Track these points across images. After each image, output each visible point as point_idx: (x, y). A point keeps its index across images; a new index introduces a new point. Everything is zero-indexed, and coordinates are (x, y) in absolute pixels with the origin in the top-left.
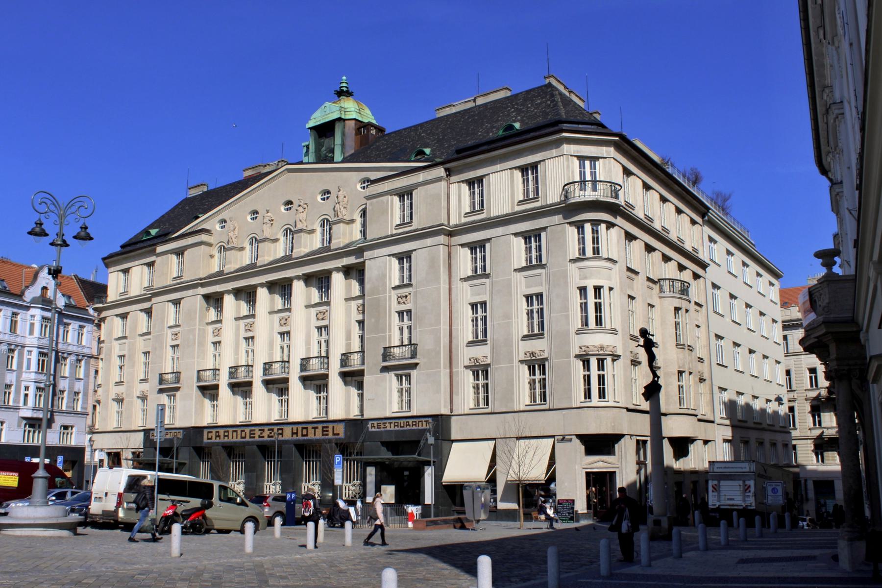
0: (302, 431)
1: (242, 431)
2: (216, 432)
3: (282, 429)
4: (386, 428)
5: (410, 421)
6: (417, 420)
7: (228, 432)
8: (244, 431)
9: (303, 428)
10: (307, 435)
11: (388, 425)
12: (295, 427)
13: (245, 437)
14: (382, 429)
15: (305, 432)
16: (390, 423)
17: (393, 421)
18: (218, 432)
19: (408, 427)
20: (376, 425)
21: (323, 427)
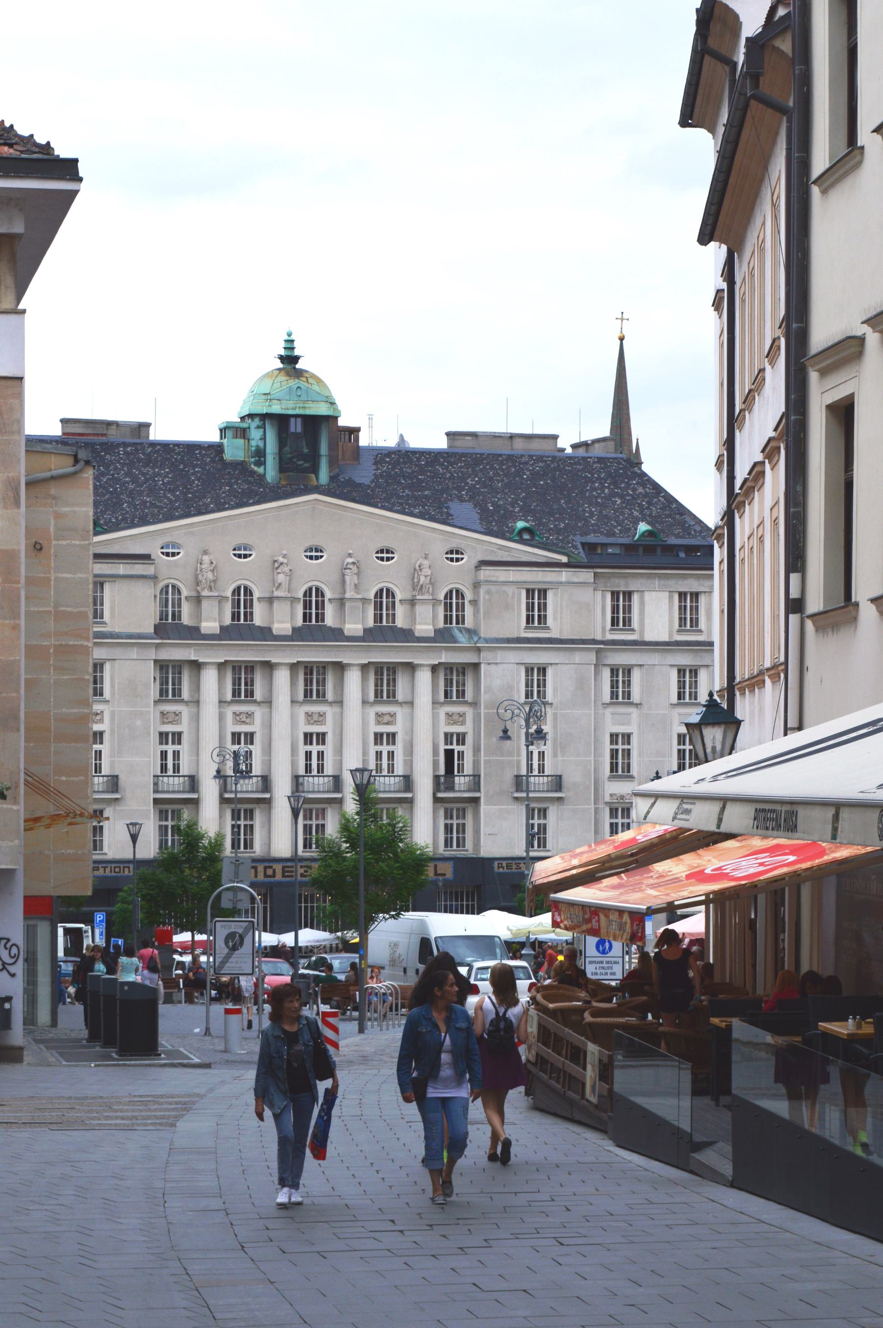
1: (265, 868)
4: (520, 868)
13: (274, 876)
14: (514, 870)
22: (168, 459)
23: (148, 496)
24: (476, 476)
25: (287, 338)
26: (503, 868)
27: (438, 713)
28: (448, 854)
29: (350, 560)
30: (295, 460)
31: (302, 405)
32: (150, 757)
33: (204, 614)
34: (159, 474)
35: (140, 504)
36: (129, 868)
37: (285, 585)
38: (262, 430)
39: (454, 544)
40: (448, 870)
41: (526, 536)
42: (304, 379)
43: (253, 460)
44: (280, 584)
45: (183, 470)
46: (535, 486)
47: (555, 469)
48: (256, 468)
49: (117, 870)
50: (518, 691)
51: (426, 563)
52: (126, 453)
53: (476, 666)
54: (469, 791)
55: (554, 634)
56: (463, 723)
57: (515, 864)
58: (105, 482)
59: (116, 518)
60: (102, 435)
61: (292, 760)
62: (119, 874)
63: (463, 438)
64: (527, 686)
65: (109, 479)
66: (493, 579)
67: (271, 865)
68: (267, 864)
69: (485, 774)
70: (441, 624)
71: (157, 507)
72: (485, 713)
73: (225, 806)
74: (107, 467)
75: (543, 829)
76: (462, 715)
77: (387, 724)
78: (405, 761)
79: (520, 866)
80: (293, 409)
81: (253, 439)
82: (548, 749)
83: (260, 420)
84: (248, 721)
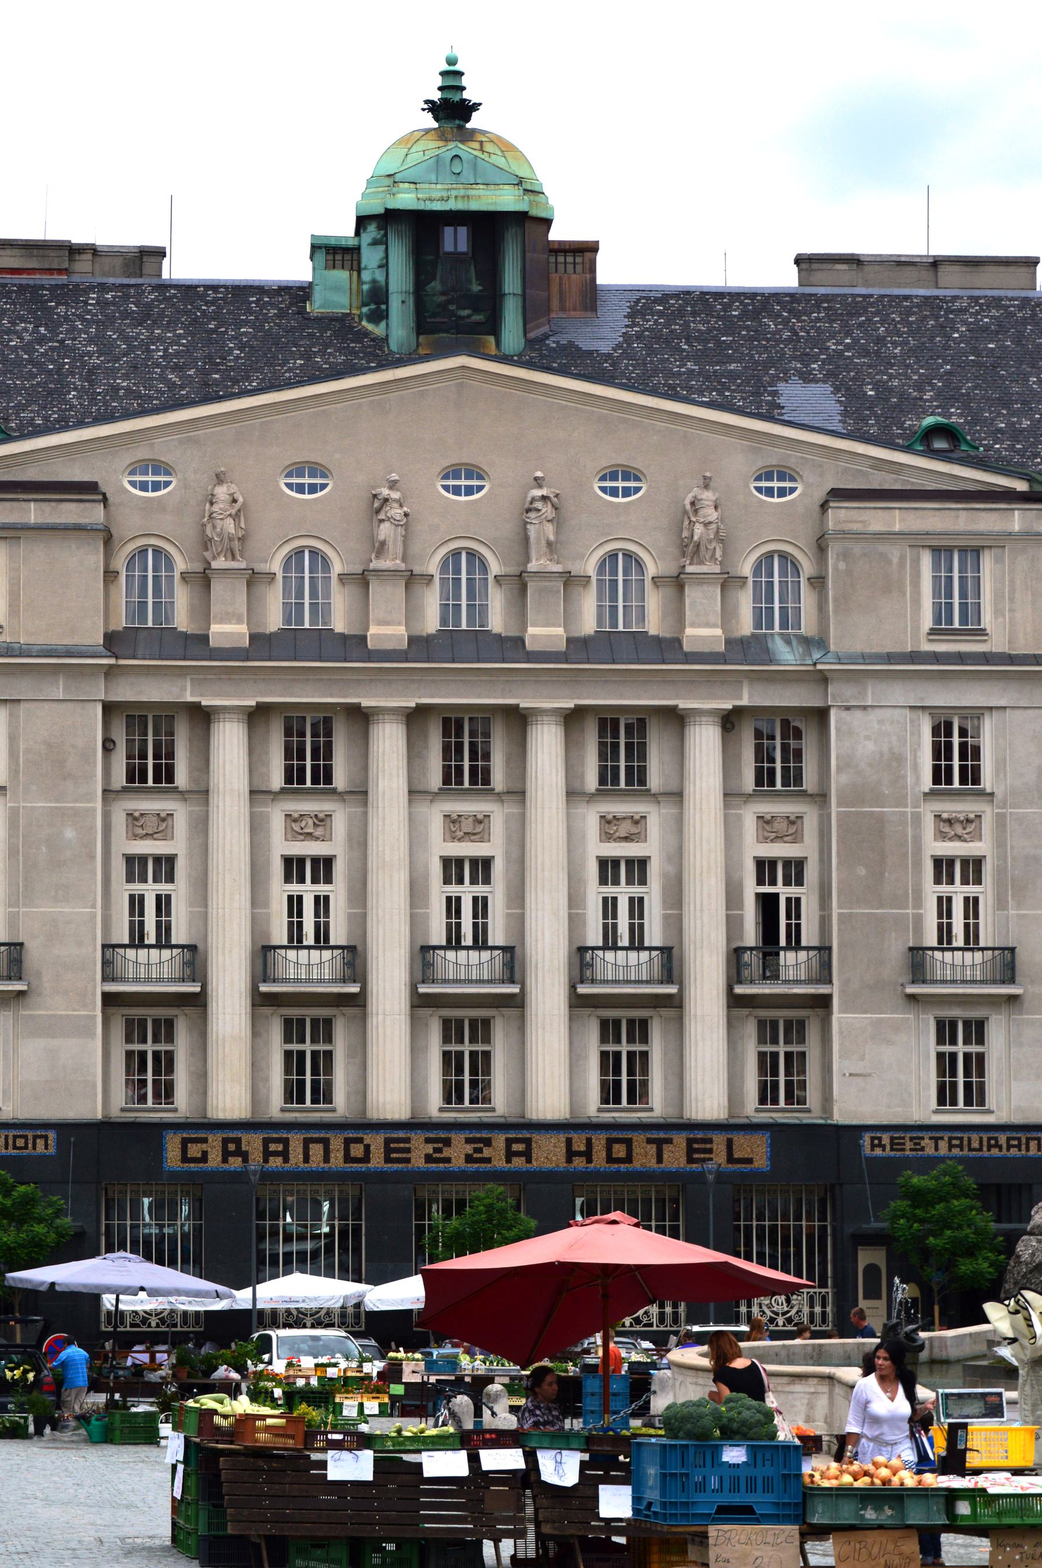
1: (348, 1142)
2: (225, 1142)
3: (528, 1142)
4: (923, 1149)
6: (1023, 1136)
7: (286, 1142)
9: (610, 1143)
10: (629, 1159)
11: (926, 1142)
13: (366, 1159)
14: (908, 1153)
15: (619, 1151)
16: (936, 1140)
17: (946, 1135)
18: (238, 1141)
19: (995, 1152)
21: (690, 1142)
22: (187, 312)
23: (126, 377)
24: (848, 334)
25: (446, 67)
26: (884, 1147)
27: (739, 817)
28: (764, 1117)
29: (538, 493)
30: (452, 307)
31: (462, 192)
32: (94, 906)
33: (215, 608)
34: (160, 339)
35: (106, 393)
36: (46, 1138)
37: (395, 547)
38: (383, 247)
39: (773, 457)
41: (940, 444)
42: (476, 145)
43: (365, 310)
44: (383, 544)
45: (213, 331)
46: (975, 351)
47: (1024, 321)
48: (370, 327)
49: (20, 1142)
50: (916, 767)
51: (708, 496)
52: (101, 303)
53: (821, 715)
54: (809, 981)
55: (996, 644)
56: (797, 838)
57: (911, 1139)
58: (42, 354)
59: (46, 419)
60: (60, 271)
61: (412, 916)
62: (25, 1152)
63: (830, 266)
64: (936, 756)
65: (52, 348)
66: (856, 527)
67: (360, 1135)
68: (351, 1135)
69: (840, 945)
70: (746, 626)
71: (139, 396)
72: (839, 813)
73: (267, 1011)
74: (53, 329)
75: (976, 1064)
76: (794, 821)
77: (626, 839)
78: (666, 918)
79: (923, 1143)
80: (442, 199)
81: (365, 268)
82: (985, 892)
83: (379, 228)
84: (319, 832)
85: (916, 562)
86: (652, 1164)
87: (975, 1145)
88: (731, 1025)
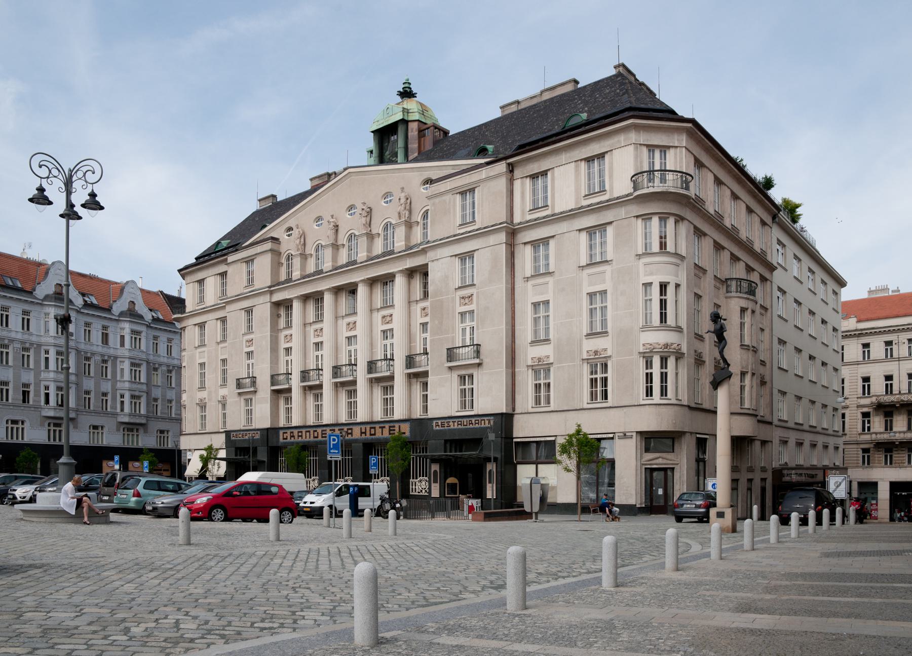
0: (370, 431)
3: (351, 429)
5: (473, 420)
7: (301, 432)
8: (316, 431)
9: (371, 428)
10: (375, 434)
11: (451, 424)
12: (363, 427)
13: (317, 437)
16: (454, 422)
17: (457, 420)
18: (293, 432)
19: (471, 425)
20: (440, 424)
21: (390, 427)
40: (406, 428)
85: (455, 200)
86: (381, 436)
87: (465, 424)
88: (410, 384)
